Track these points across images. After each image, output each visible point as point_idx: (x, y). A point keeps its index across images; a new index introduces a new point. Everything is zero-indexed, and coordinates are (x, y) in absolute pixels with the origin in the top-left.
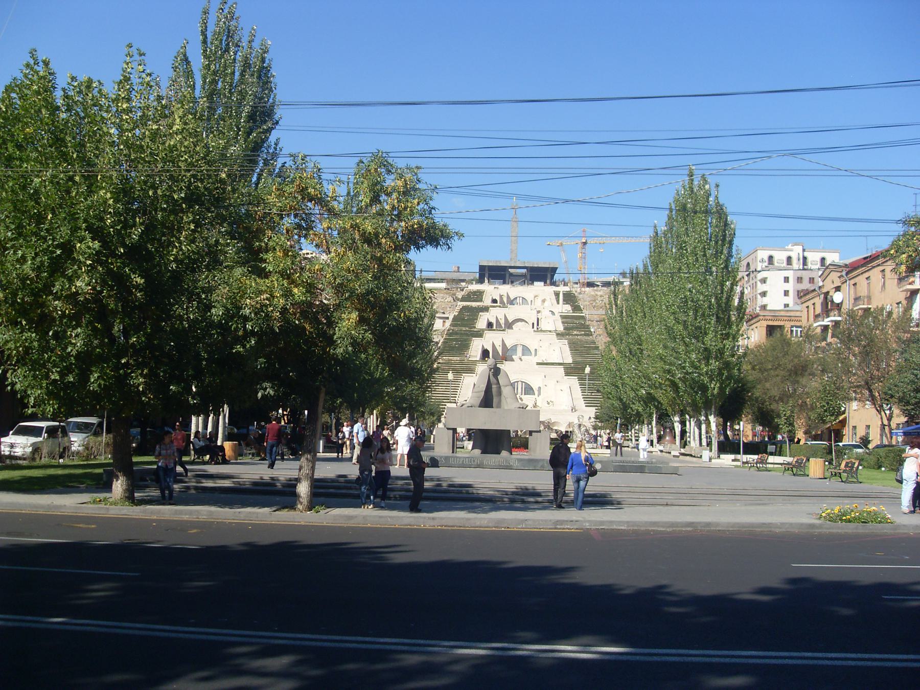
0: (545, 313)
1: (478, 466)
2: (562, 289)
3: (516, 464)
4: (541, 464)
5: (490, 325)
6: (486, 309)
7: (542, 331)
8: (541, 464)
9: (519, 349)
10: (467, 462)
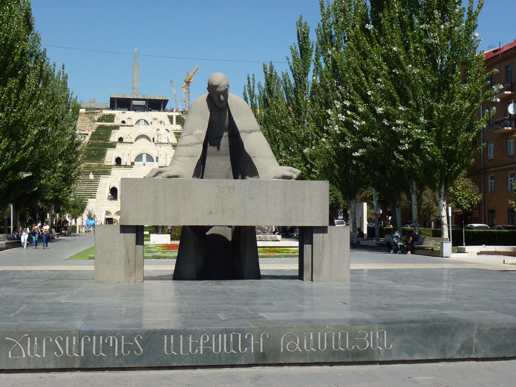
0: (163, 131)
1: (262, 360)
2: (175, 114)
3: (383, 344)
4: (461, 339)
5: (121, 140)
6: (117, 127)
7: (161, 143)
8: (461, 339)
9: (144, 157)
10: (221, 346)
